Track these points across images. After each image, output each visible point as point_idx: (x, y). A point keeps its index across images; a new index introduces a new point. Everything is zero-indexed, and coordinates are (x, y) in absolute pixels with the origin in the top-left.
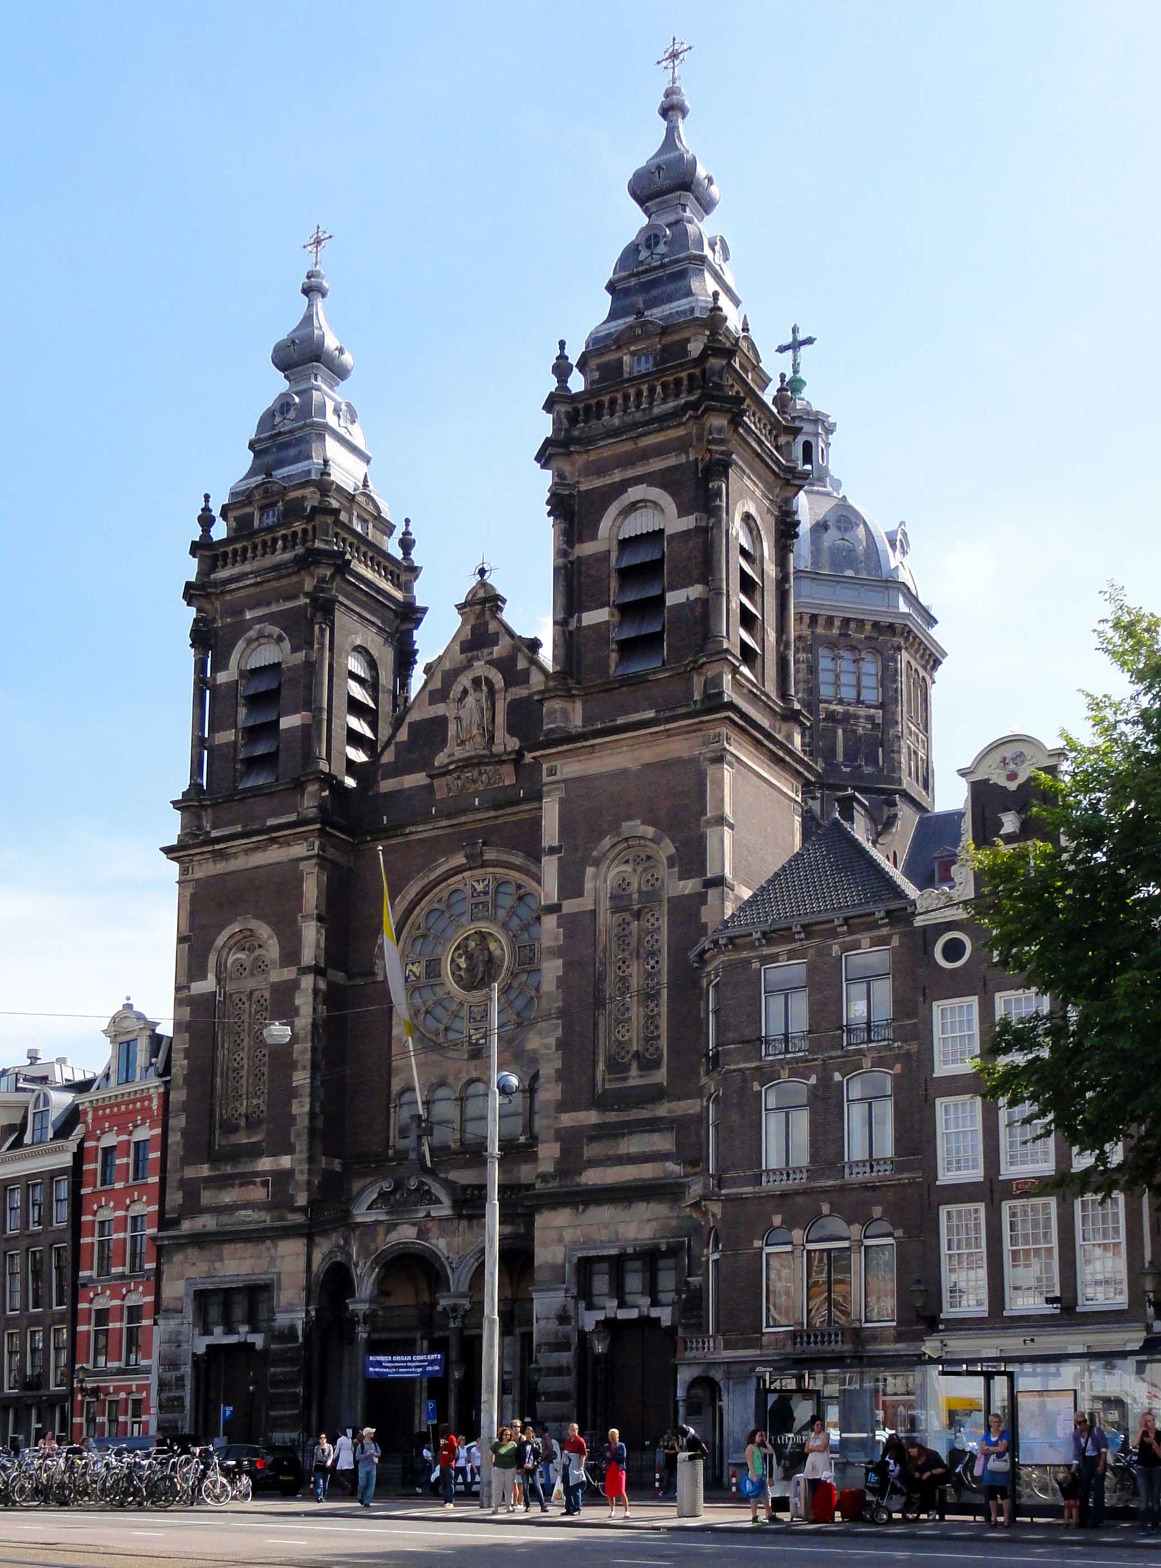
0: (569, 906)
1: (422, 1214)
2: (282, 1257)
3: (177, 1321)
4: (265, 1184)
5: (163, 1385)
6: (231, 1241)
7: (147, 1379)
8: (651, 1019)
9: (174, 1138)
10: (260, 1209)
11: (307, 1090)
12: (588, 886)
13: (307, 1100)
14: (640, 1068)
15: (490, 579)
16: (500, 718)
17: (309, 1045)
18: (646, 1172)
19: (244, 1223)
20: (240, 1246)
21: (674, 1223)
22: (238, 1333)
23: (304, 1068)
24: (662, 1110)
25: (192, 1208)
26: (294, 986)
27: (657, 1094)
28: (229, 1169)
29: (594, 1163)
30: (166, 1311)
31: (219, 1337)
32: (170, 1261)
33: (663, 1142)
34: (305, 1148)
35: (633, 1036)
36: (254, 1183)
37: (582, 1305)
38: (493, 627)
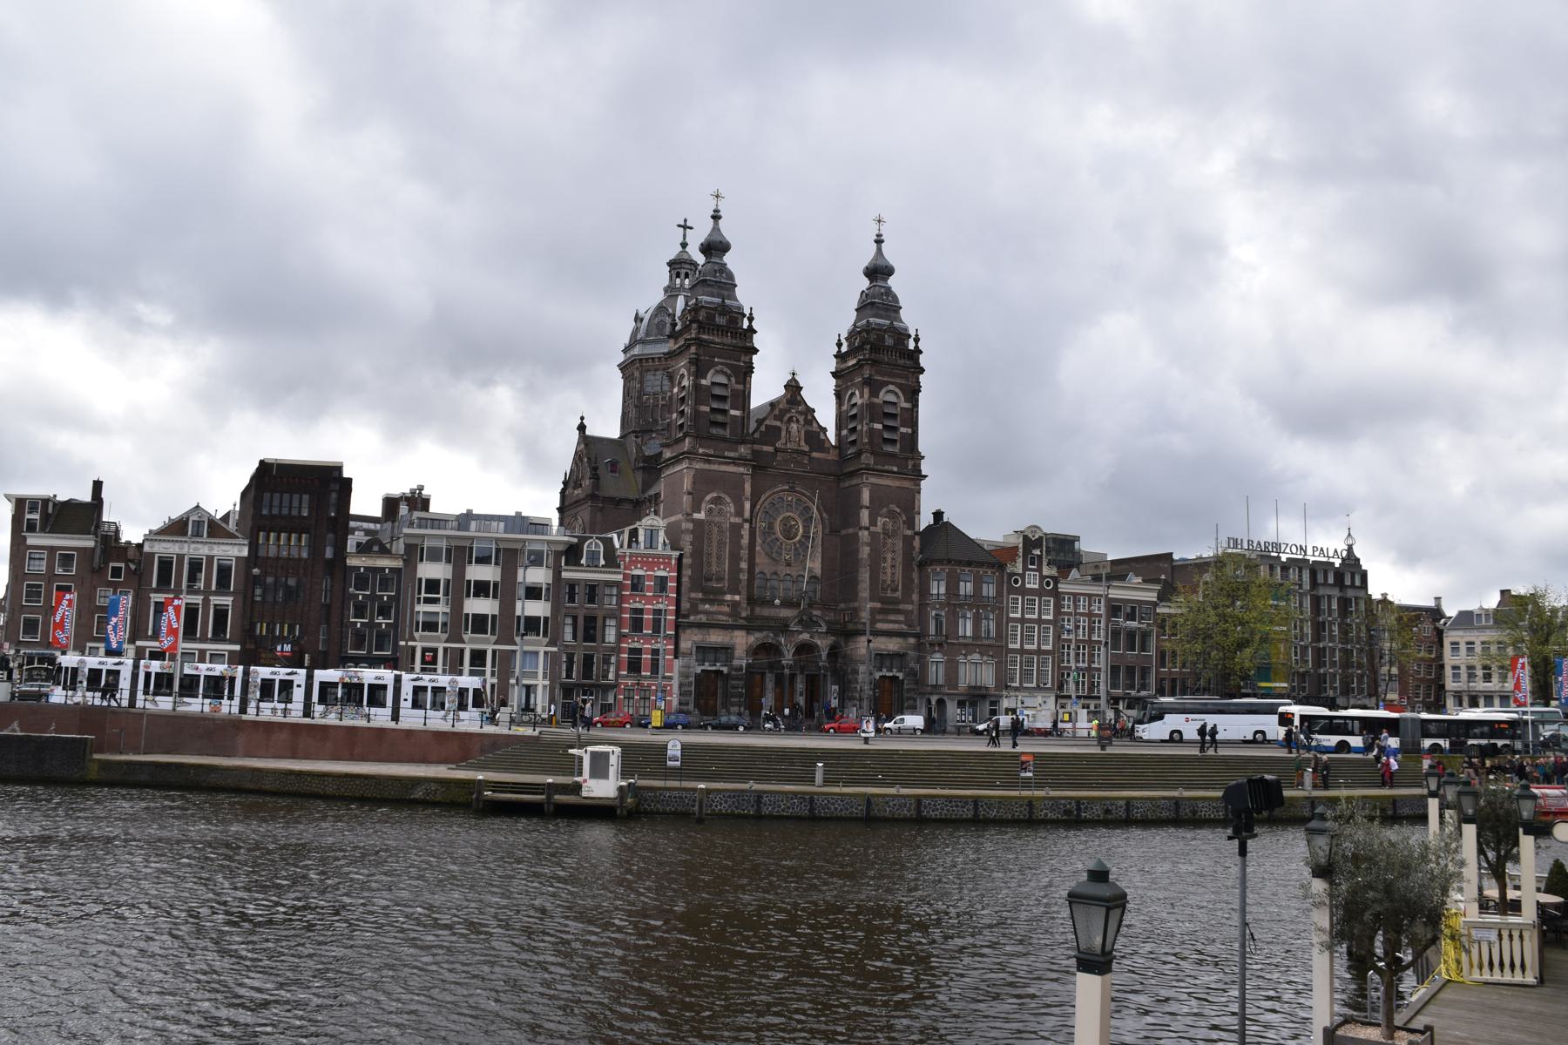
0: (872, 529)
5: (681, 685)
8: (893, 574)
9: (685, 579)
13: (746, 574)
16: (803, 437)
18: (896, 626)
24: (901, 607)
25: (694, 610)
26: (741, 526)
27: (896, 602)
28: (712, 597)
29: (880, 621)
31: (707, 667)
33: (901, 618)
38: (799, 398)
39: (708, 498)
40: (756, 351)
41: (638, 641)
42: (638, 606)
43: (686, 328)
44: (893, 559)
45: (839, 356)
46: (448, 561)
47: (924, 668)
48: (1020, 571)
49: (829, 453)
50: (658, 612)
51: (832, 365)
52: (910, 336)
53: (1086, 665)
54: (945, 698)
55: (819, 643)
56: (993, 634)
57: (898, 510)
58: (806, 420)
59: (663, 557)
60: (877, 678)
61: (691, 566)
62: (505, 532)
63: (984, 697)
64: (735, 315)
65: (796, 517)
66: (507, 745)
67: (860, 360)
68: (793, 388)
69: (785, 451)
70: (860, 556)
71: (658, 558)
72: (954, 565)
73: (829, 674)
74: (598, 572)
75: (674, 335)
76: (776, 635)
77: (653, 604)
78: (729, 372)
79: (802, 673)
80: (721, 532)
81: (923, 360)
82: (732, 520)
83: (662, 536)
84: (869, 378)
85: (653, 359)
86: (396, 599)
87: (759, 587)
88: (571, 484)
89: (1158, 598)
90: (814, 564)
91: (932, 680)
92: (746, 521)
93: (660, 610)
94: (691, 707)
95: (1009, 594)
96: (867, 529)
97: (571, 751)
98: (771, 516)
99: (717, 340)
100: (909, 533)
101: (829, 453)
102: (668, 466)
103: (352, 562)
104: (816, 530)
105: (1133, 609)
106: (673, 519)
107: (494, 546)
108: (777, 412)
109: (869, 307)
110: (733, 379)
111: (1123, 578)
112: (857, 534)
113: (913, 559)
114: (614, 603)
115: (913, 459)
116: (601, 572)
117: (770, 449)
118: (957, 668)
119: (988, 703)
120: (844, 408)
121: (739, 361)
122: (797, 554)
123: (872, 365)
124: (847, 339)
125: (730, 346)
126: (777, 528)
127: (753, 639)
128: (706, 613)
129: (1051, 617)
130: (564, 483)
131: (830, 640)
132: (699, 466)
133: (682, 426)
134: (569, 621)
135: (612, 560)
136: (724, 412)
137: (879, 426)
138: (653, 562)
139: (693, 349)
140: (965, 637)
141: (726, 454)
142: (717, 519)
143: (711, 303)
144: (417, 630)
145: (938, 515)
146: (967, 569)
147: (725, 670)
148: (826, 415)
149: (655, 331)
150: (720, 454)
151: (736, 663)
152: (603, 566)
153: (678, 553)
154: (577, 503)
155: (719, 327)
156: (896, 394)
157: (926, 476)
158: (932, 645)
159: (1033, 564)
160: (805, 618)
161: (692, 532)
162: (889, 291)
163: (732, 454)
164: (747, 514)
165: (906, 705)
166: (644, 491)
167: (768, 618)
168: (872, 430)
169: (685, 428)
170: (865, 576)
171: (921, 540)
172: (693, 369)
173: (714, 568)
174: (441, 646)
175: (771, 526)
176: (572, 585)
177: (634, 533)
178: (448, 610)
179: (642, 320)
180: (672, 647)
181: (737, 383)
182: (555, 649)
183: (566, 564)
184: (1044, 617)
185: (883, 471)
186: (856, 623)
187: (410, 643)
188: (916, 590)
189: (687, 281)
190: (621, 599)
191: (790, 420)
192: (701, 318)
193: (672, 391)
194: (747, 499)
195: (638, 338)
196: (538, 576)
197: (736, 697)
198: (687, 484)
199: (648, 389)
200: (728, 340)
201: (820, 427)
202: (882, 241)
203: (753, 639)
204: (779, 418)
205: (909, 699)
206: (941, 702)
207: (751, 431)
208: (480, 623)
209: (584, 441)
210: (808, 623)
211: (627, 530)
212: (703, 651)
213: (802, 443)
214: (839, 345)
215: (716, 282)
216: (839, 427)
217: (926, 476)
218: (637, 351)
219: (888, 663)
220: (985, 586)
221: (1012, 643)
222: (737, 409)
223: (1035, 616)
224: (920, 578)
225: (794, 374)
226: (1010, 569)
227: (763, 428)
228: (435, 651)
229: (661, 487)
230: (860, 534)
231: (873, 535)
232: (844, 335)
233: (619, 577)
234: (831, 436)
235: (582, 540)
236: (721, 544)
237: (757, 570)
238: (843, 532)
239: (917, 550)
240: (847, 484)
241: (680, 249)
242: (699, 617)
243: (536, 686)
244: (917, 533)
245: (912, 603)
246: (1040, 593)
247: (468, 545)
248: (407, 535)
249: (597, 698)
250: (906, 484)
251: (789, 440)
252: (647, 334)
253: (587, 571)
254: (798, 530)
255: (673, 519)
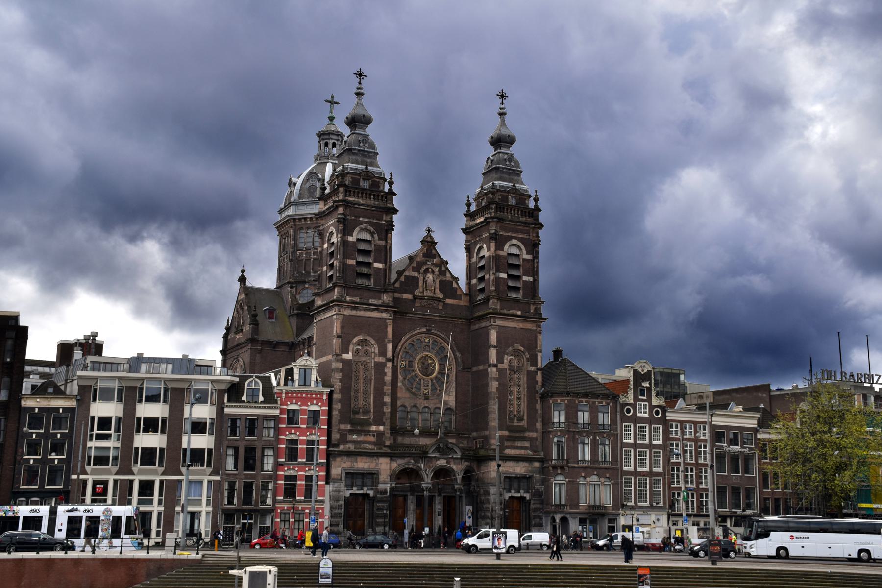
0: (500, 366)
1: (450, 456)
2: (381, 463)
3: (339, 484)
4: (374, 435)
5: (332, 508)
6: (361, 455)
7: (323, 505)
8: (519, 405)
9: (335, 413)
10: (372, 445)
11: (390, 404)
12: (505, 361)
13: (389, 407)
14: (517, 420)
15: (432, 234)
16: (437, 285)
17: (390, 387)
18: (522, 452)
19: (366, 449)
20: (364, 457)
21: (530, 469)
22: (363, 489)
23: (388, 395)
24: (527, 434)
25: (344, 440)
26: (383, 365)
27: (522, 430)
28: (359, 428)
30: (334, 479)
31: (355, 491)
32: (335, 460)
34: (389, 424)
35: (515, 409)
36: (370, 435)
37: (505, 491)
38: (434, 252)
39: (355, 340)
40: (395, 211)
41: (293, 469)
42: (293, 437)
43: (334, 192)
44: (518, 392)
45: (470, 215)
46: (120, 400)
47: (549, 489)
48: (632, 402)
49: (461, 299)
50: (311, 442)
51: (463, 222)
52: (530, 196)
53: (694, 486)
54: (568, 516)
55: (454, 467)
56: (609, 458)
57: (522, 349)
58: (440, 271)
59: (316, 393)
60: (507, 498)
61: (340, 401)
62: (173, 373)
63: (603, 515)
64: (376, 180)
65: (433, 356)
66: (172, 569)
67: (487, 218)
68: (429, 243)
69: (422, 298)
70: (490, 390)
71: (312, 394)
72: (573, 397)
73: (463, 495)
74: (258, 407)
75: (323, 198)
76: (416, 461)
77: (307, 436)
78: (372, 229)
79: (440, 495)
80: (367, 370)
81: (542, 217)
82: (377, 359)
83: (314, 375)
84: (495, 233)
85: (305, 219)
86: (70, 436)
87: (400, 419)
88: (233, 330)
89: (758, 425)
90: (449, 398)
91: (555, 500)
92: (388, 360)
93: (313, 441)
94: (341, 528)
95: (622, 422)
96: (495, 366)
97: (231, 572)
98: (411, 356)
99: (361, 202)
100: (532, 368)
101: (461, 299)
102: (319, 312)
103: (26, 403)
104: (451, 367)
105: (736, 435)
106: (324, 359)
107: (162, 386)
108: (414, 264)
109: (494, 171)
110: (376, 236)
111: (725, 406)
112: (486, 370)
113: (536, 392)
114: (272, 435)
115: (534, 303)
116: (260, 407)
117: (409, 297)
118: (578, 489)
119: (606, 521)
120: (474, 260)
121: (381, 220)
122: (434, 389)
123: (497, 222)
124: (475, 200)
125: (372, 207)
126: (416, 366)
127: (395, 465)
128: (354, 442)
129: (660, 443)
130: (226, 328)
131: (464, 465)
132: (347, 312)
133: (331, 277)
134: (231, 452)
135: (270, 396)
136: (369, 265)
137: (504, 276)
138: (306, 398)
139: (341, 210)
140: (584, 461)
141: (371, 301)
142: (363, 359)
143: (356, 169)
144: (89, 464)
145: (557, 353)
146: (584, 400)
147: (371, 493)
148: (458, 266)
149: (306, 194)
150: (365, 301)
151: (381, 487)
152: (262, 402)
153: (328, 389)
154: (239, 346)
155: (363, 190)
156: (519, 247)
157: (546, 319)
158: (554, 468)
159: (642, 395)
160: (441, 445)
161: (341, 371)
162: (511, 158)
163: (376, 302)
164: (389, 354)
165: (533, 523)
166: (298, 335)
167: (410, 446)
168: (498, 280)
169: (334, 279)
170: (494, 407)
171: (543, 375)
172: (341, 227)
173: (361, 403)
174: (111, 479)
175: (411, 364)
176: (234, 419)
177: (289, 373)
178: (119, 445)
179: (295, 184)
180: (324, 474)
181: (380, 239)
182: (218, 478)
183: (229, 401)
184: (654, 443)
185: (508, 315)
186: (486, 450)
187: (82, 477)
188: (539, 420)
189: (334, 150)
190: (278, 431)
191: (427, 271)
192: (347, 183)
193: (323, 247)
194: (389, 341)
195: (292, 200)
196: (203, 412)
197: (381, 517)
198: (336, 328)
199: (301, 245)
200: (371, 202)
201: (452, 277)
202: (505, 114)
203: (395, 465)
204: (417, 269)
205: (535, 517)
206: (564, 520)
207: (392, 281)
208: (148, 456)
209: (244, 292)
210: (444, 450)
211: (283, 370)
212: (352, 477)
213: (437, 291)
214: (469, 205)
215: (360, 151)
216: (469, 277)
217: (546, 319)
218: (291, 211)
219: (516, 485)
220: (600, 415)
221: (626, 466)
222: (380, 262)
223: (647, 442)
224: (543, 408)
225: (429, 231)
226: (622, 400)
227: (403, 279)
228: (105, 483)
229: (313, 331)
230: (489, 370)
231: (500, 371)
232: (473, 196)
233: (277, 412)
234: (463, 284)
235: (243, 379)
236: (367, 381)
237: (399, 403)
238: (474, 369)
239: (540, 383)
240: (477, 326)
241: (327, 121)
242: (347, 446)
243: (200, 512)
244: (539, 369)
245: (536, 431)
246: (650, 421)
247: (139, 386)
248: (80, 378)
249: (256, 522)
250: (529, 326)
251: (425, 288)
252: (300, 197)
253: (247, 407)
254: (434, 367)
255: (324, 359)
